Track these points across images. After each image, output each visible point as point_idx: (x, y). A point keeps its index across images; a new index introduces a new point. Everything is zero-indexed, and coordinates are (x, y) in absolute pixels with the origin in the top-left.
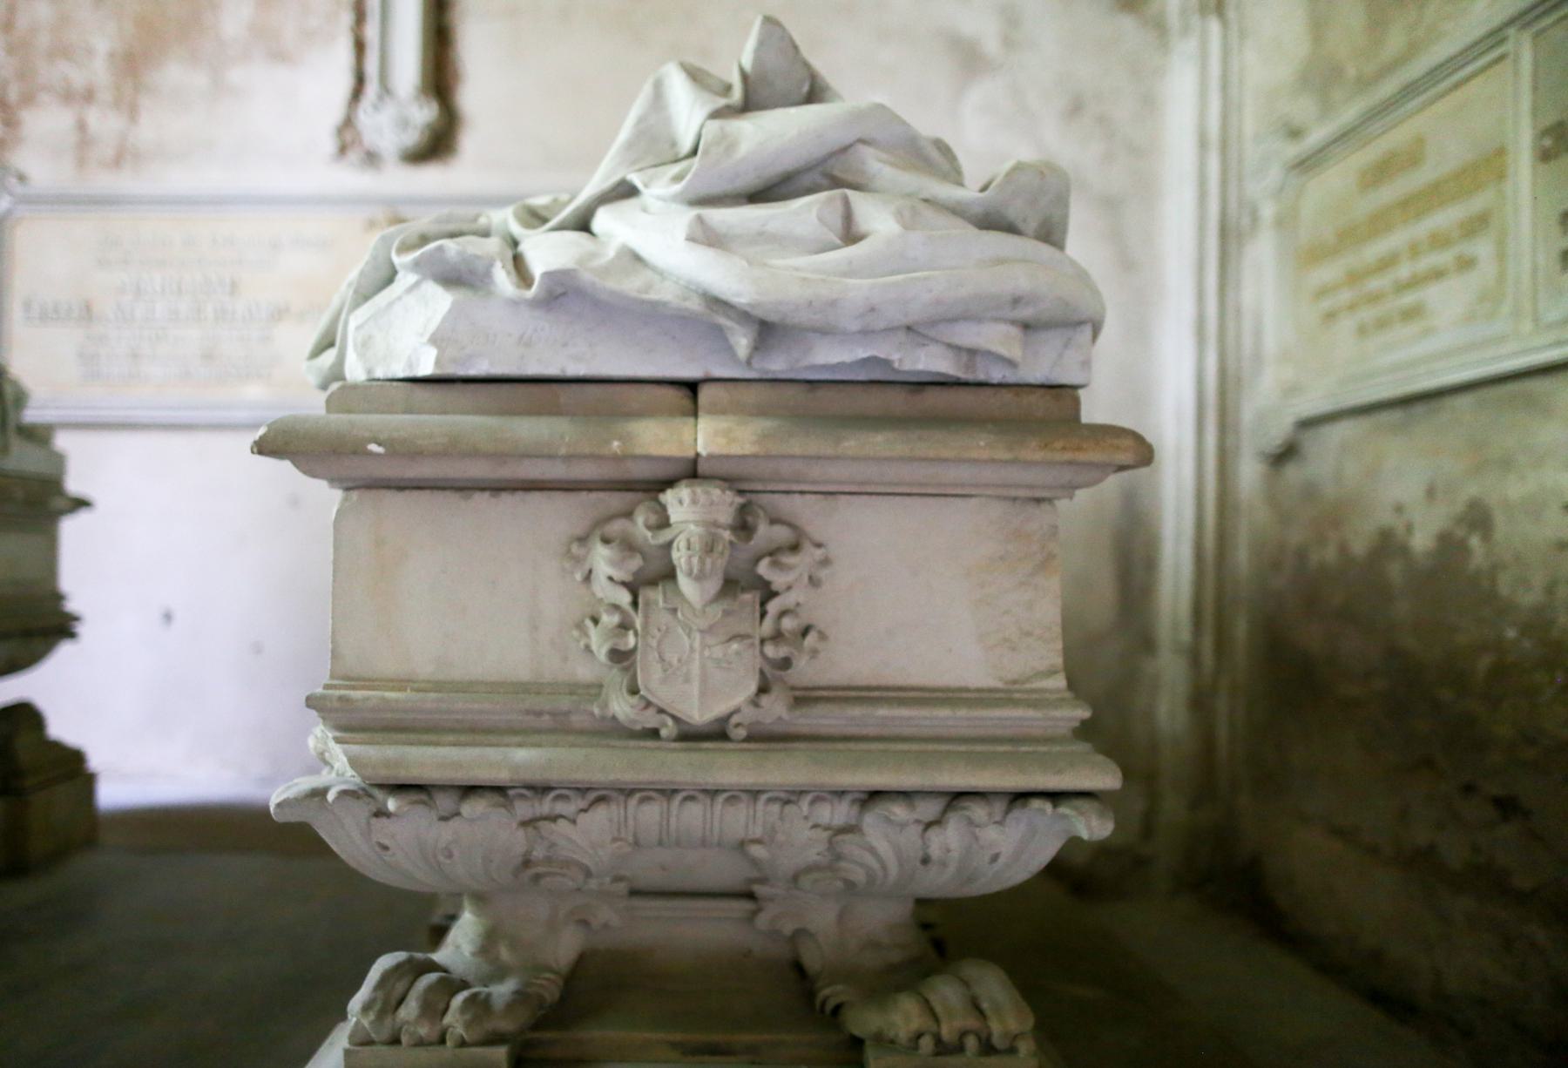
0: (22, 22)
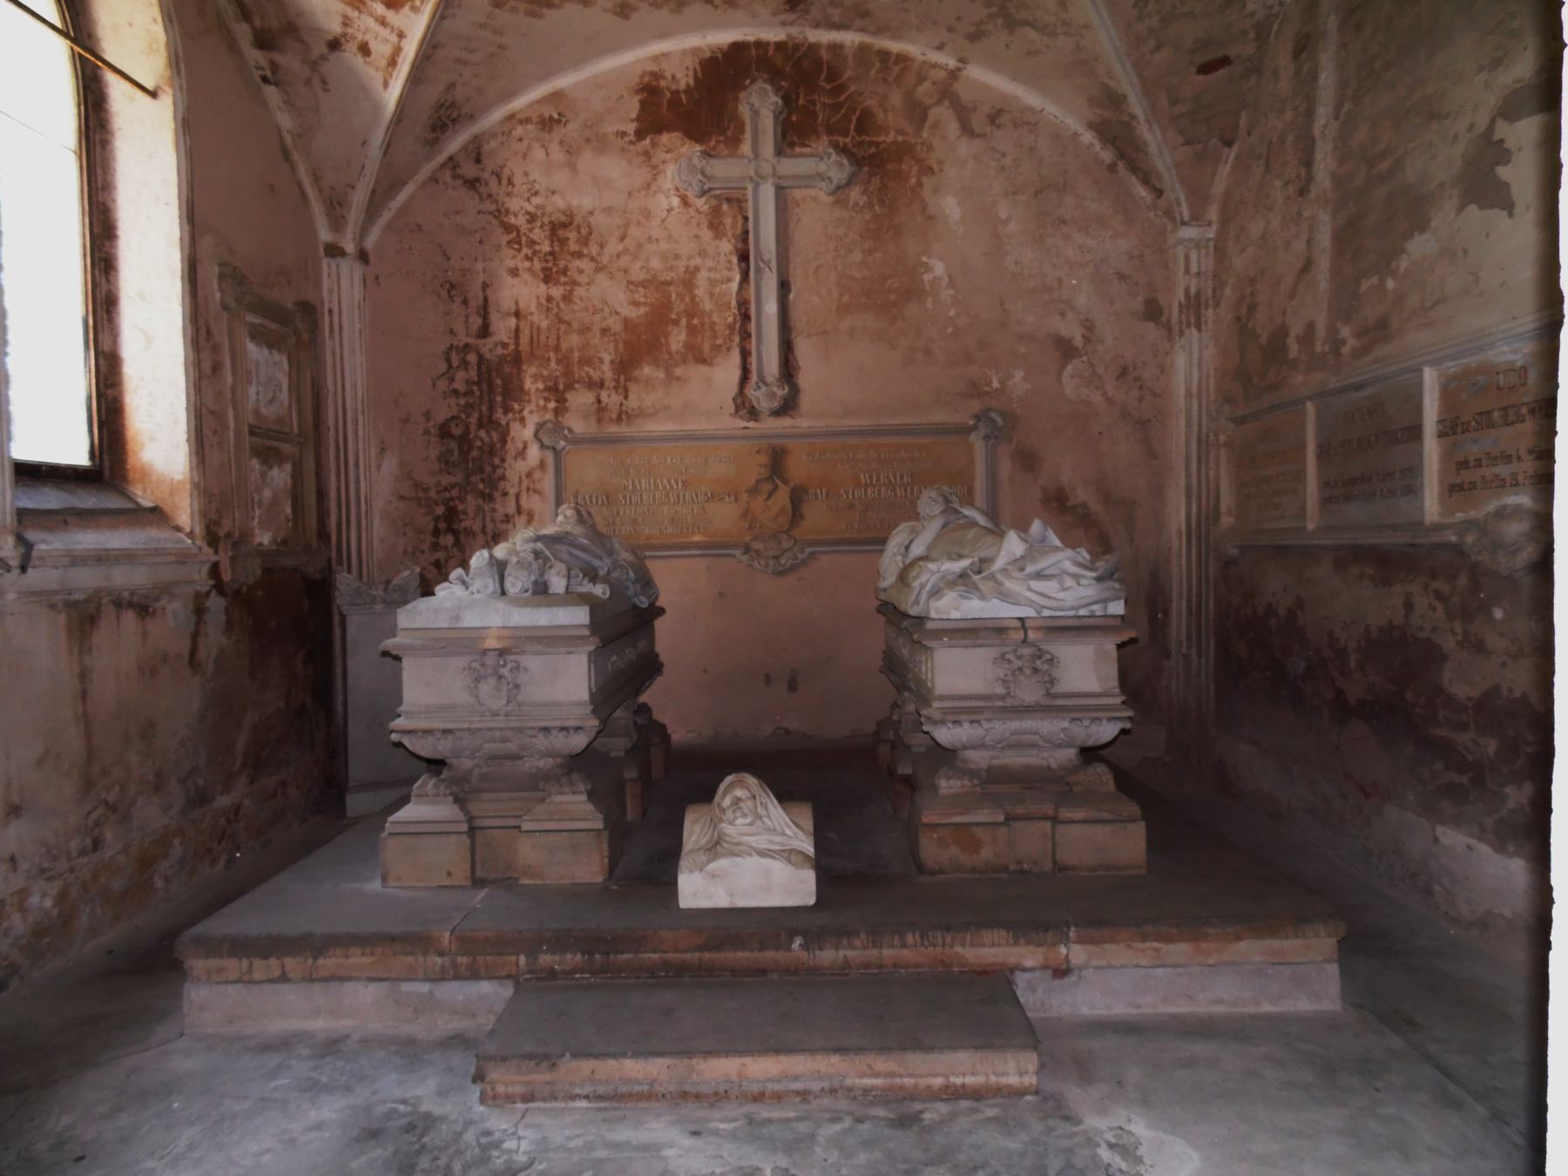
0: (564, 346)
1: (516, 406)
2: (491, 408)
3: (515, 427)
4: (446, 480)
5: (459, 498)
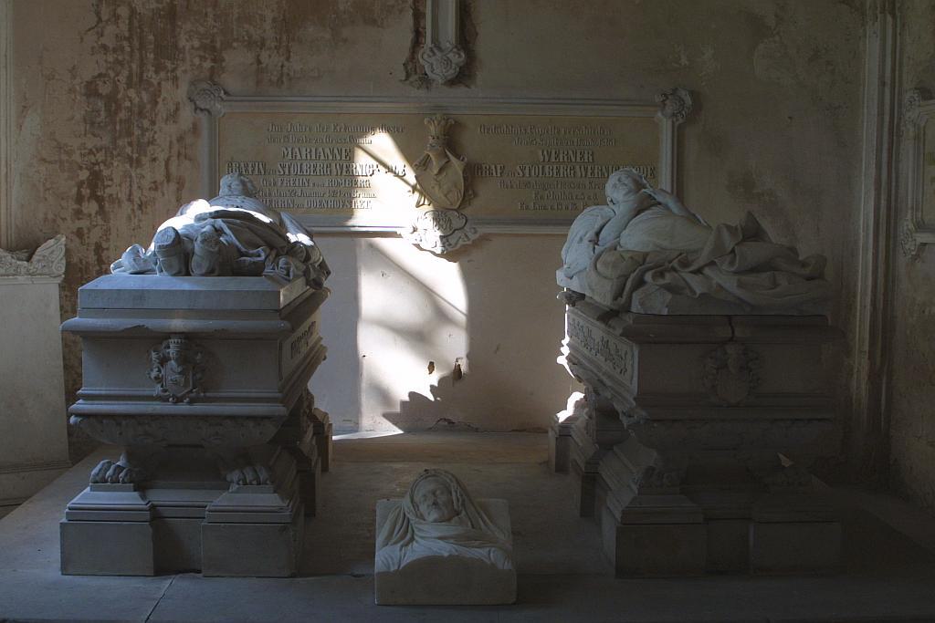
1: (169, 65)
2: (142, 65)
3: (167, 86)
4: (91, 143)
5: (104, 162)
